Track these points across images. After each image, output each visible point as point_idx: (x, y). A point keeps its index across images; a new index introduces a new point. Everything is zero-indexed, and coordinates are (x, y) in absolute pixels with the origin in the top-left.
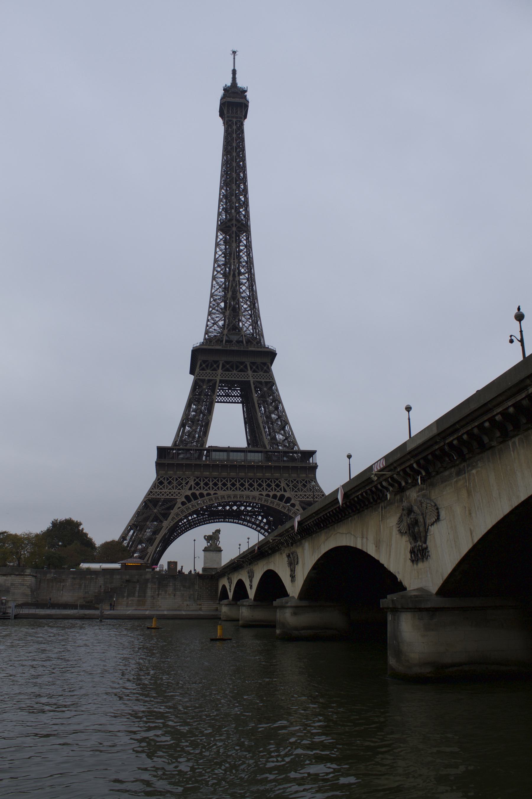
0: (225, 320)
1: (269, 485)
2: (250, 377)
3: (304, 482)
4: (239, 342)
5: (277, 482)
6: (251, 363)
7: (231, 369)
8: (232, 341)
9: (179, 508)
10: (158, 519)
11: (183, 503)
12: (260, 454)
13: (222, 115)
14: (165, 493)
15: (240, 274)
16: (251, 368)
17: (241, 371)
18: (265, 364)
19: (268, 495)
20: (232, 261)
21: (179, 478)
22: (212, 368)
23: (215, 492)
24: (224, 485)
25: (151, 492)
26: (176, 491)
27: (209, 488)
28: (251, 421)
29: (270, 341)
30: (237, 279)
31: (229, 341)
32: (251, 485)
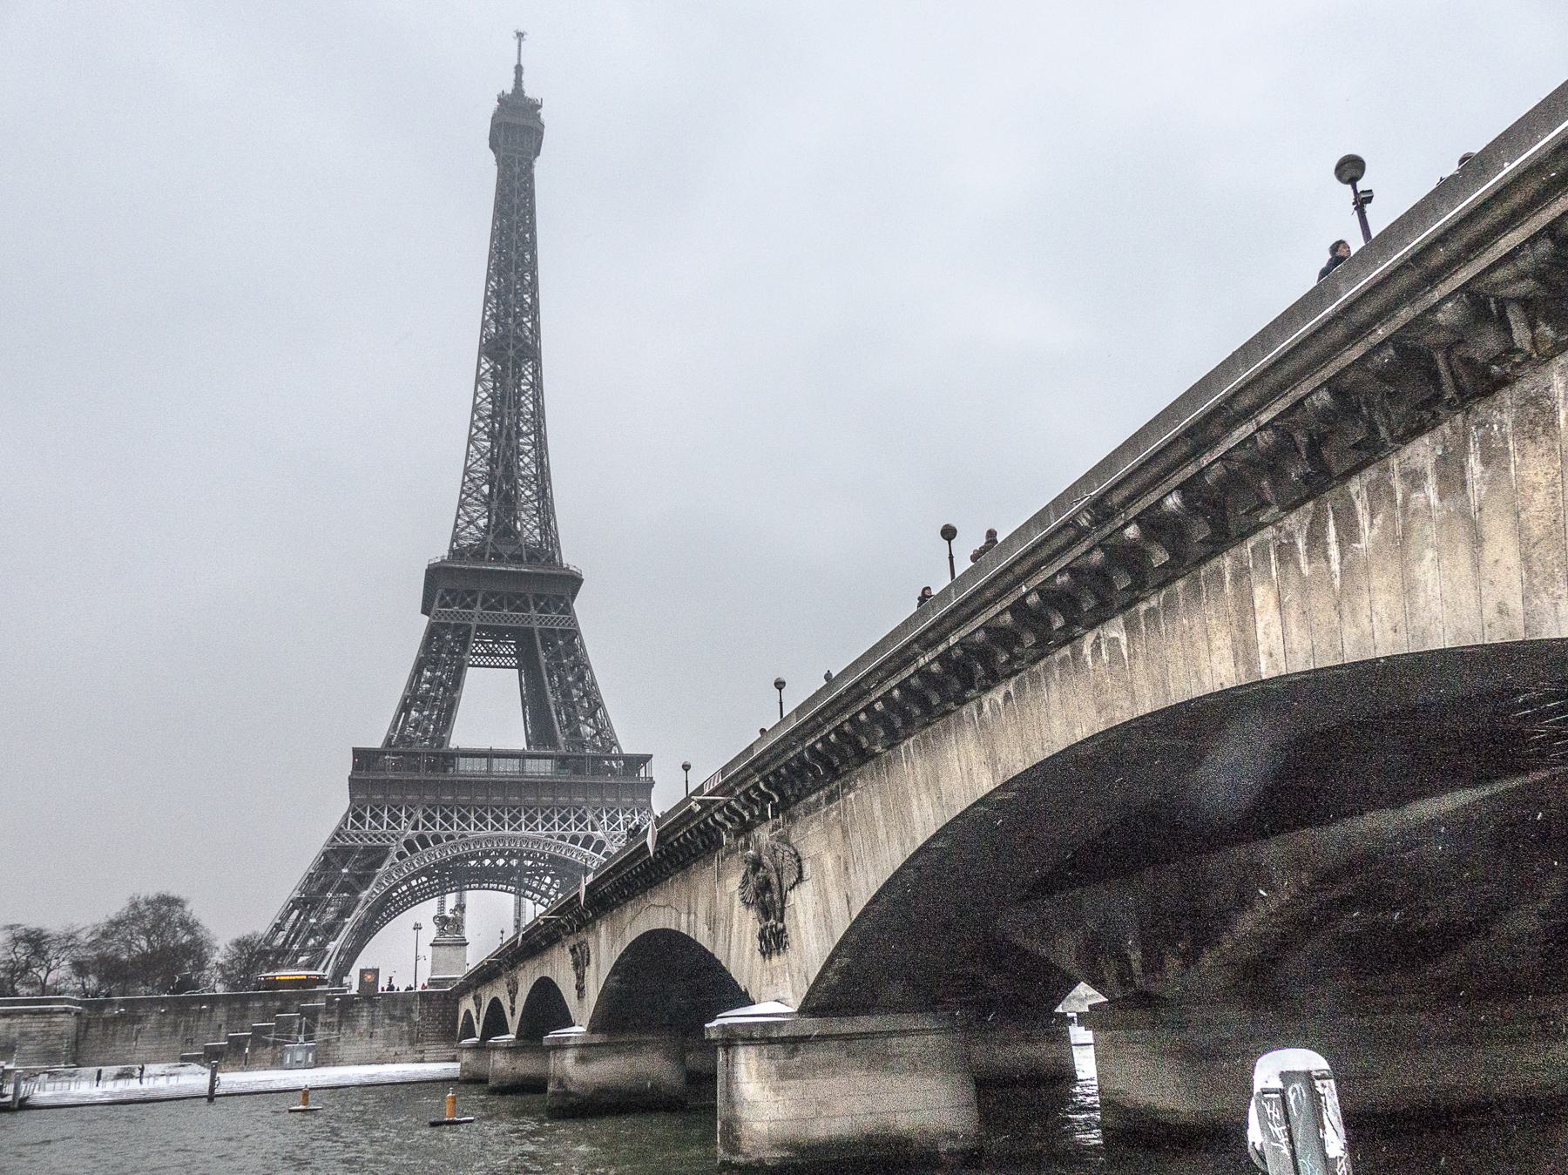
0: (489, 517)
2: (535, 620)
10: (346, 883)
11: (401, 856)
12: (549, 762)
13: (494, 145)
15: (520, 434)
16: (536, 605)
17: (518, 609)
18: (561, 598)
20: (506, 410)
28: (534, 702)
29: (570, 557)
30: (514, 443)
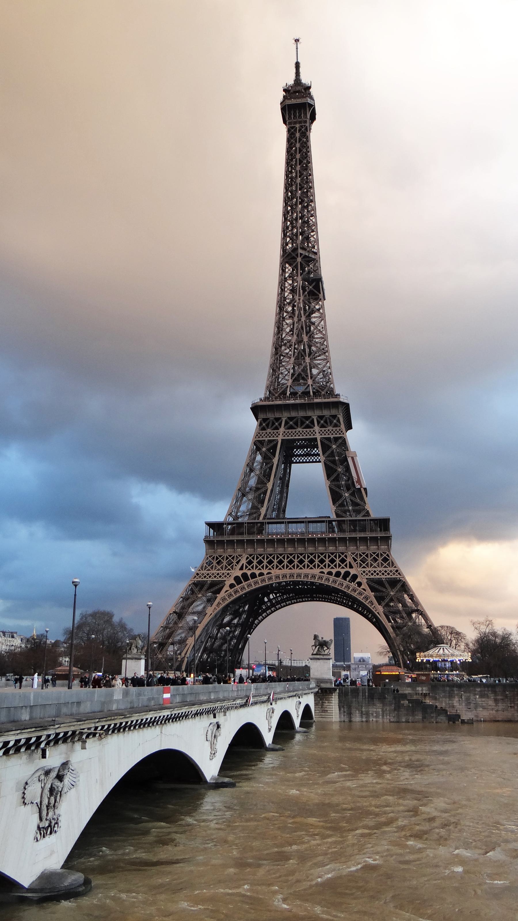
1: (333, 561)
3: (374, 556)
4: (306, 394)
5: (343, 556)
7: (296, 427)
8: (297, 393)
9: (227, 591)
14: (213, 574)
16: (318, 423)
17: (308, 427)
18: (334, 417)
19: (330, 573)
21: (230, 556)
22: (275, 426)
24: (280, 562)
25: (198, 574)
26: (224, 571)
27: (263, 567)
32: (312, 561)
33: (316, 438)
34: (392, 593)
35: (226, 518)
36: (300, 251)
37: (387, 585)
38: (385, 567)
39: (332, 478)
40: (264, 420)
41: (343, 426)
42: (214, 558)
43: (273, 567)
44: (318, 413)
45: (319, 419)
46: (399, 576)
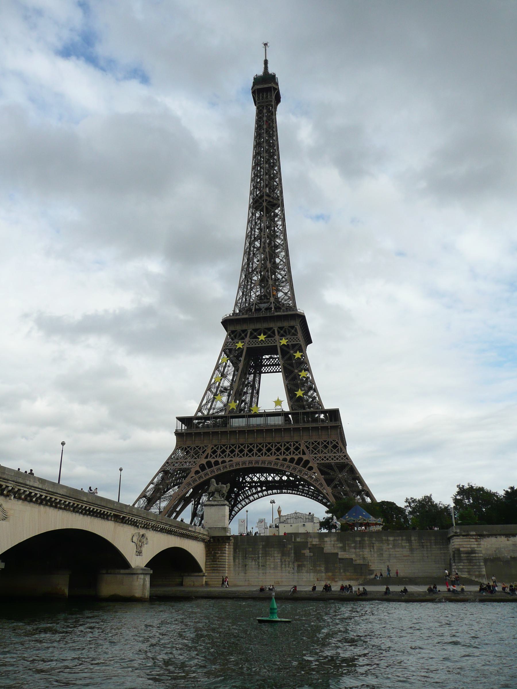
1: (287, 449)
3: (325, 443)
4: (268, 309)
5: (297, 445)
6: (279, 327)
9: (191, 477)
12: (280, 417)
16: (279, 332)
18: (292, 327)
19: (285, 460)
21: (197, 447)
23: (231, 459)
27: (225, 456)
31: (258, 310)
32: (269, 450)
33: (276, 345)
34: (340, 476)
35: (197, 413)
36: (265, 197)
37: (336, 468)
38: (335, 453)
39: (290, 377)
40: (233, 332)
41: (300, 335)
42: (183, 449)
43: (234, 456)
44: (279, 324)
45: (279, 330)
46: (347, 461)
